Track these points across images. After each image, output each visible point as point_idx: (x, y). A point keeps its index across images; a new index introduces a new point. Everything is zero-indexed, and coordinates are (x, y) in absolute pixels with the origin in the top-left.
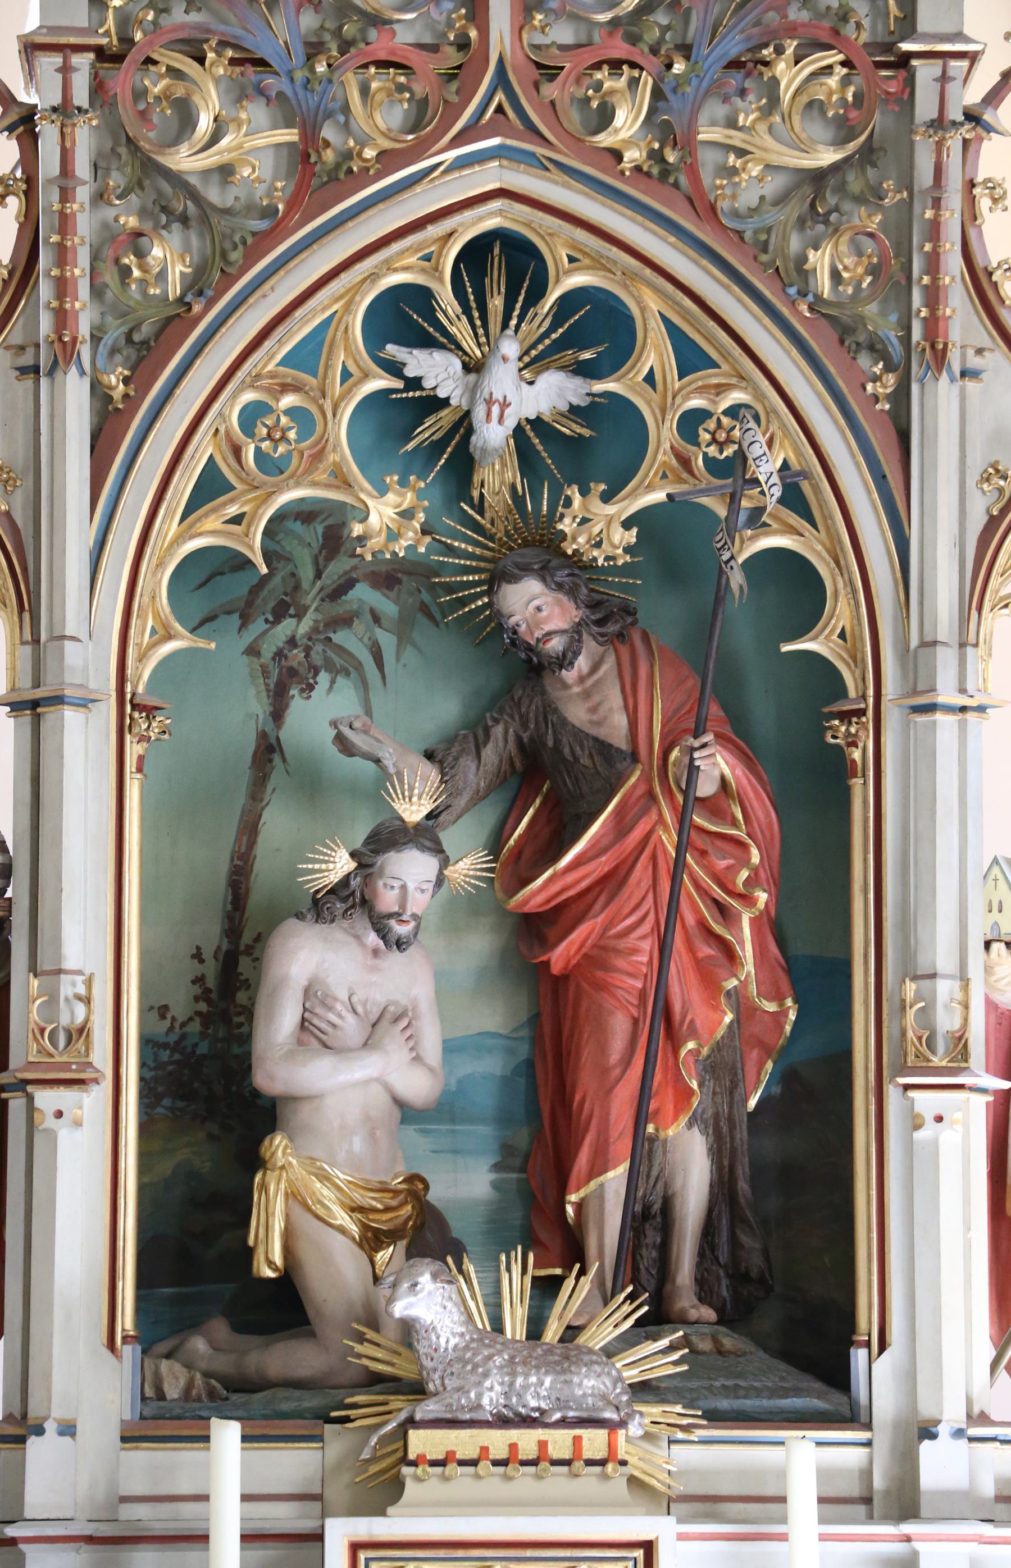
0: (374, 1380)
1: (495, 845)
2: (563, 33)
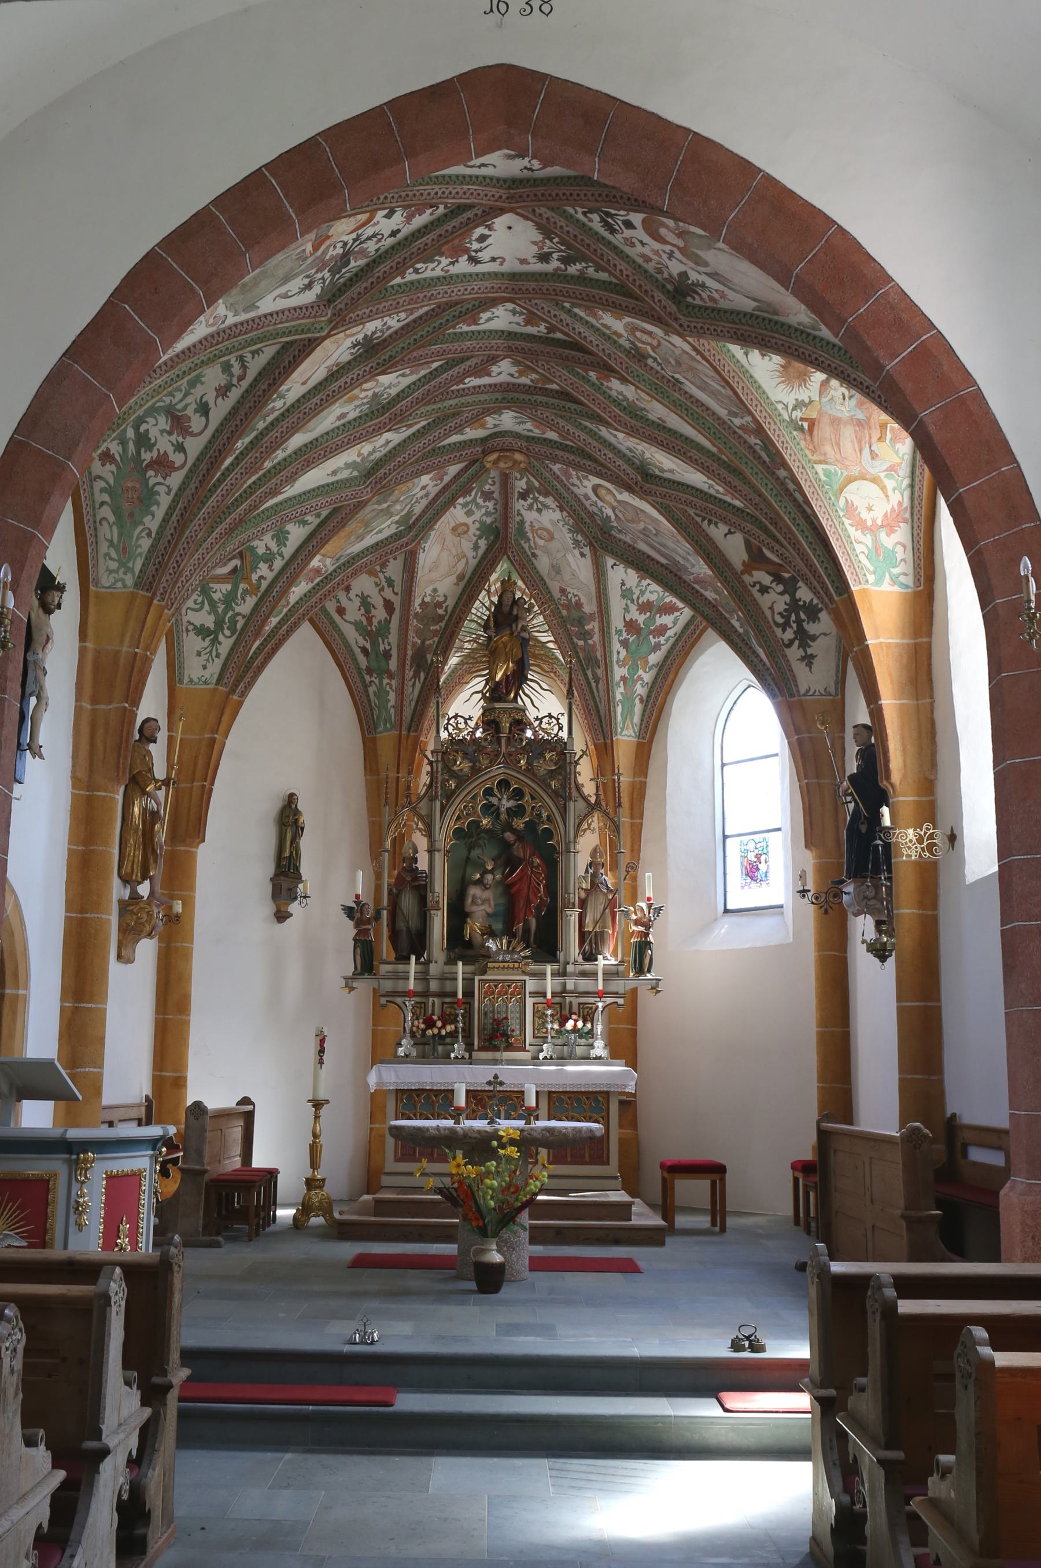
0: (483, 956)
1: (503, 873)
2: (513, 749)
